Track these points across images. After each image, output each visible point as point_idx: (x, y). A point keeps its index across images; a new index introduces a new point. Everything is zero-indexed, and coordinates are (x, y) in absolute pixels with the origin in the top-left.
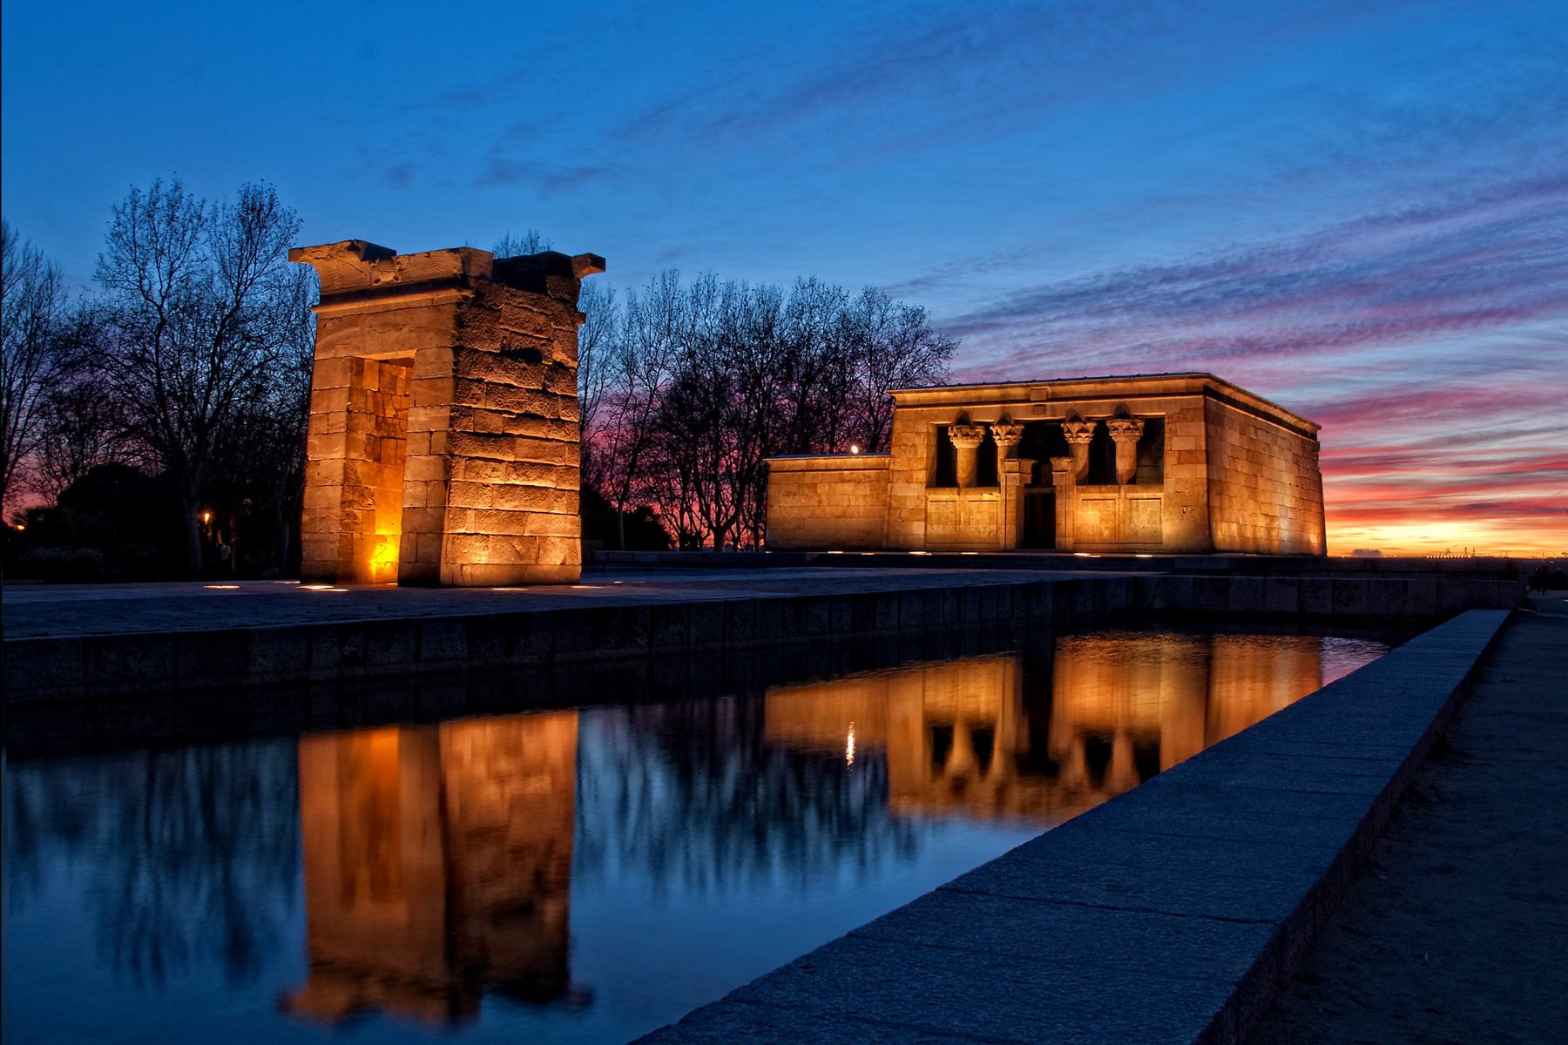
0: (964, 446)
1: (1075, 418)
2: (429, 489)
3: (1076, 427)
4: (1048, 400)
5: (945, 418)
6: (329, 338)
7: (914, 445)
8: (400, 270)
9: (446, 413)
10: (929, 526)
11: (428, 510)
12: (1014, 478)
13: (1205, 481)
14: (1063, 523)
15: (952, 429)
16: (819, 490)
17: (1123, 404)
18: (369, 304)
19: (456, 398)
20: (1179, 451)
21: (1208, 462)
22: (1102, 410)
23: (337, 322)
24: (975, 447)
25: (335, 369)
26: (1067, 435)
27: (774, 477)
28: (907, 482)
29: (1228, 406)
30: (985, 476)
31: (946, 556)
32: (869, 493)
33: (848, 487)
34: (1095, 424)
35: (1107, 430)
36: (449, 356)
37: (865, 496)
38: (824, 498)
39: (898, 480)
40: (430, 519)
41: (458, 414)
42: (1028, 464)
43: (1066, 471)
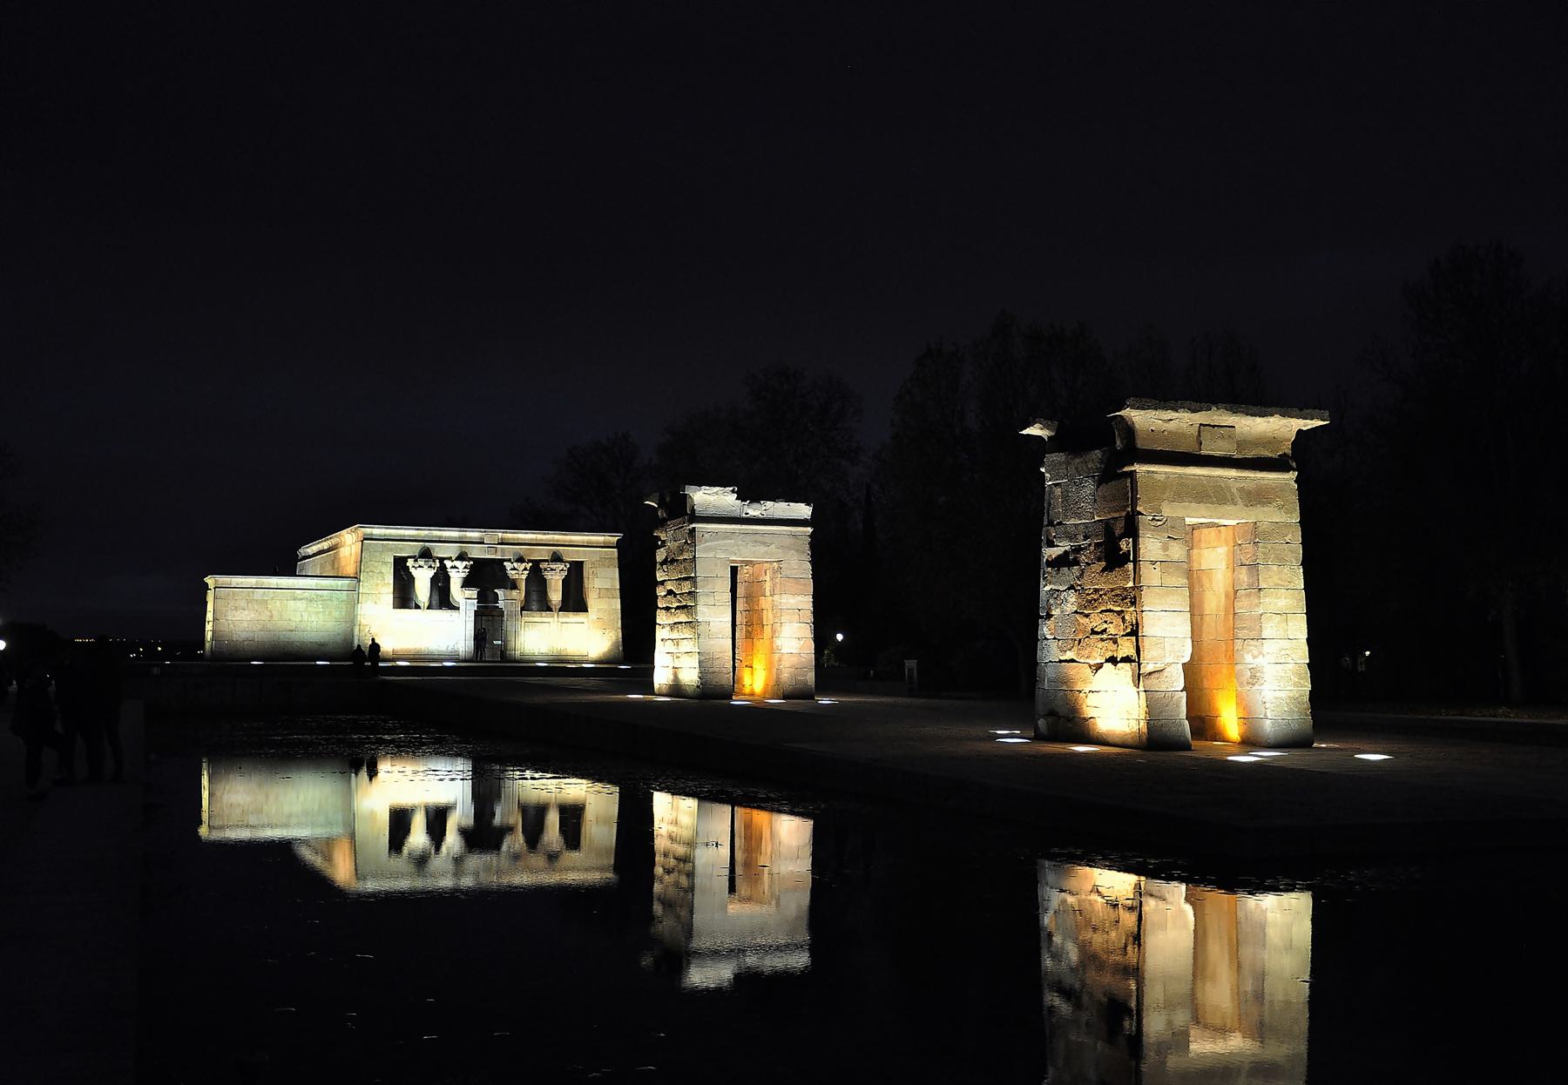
0: (423, 577)
1: (521, 560)
2: (802, 642)
4: (499, 544)
6: (707, 544)
12: (474, 604)
14: (513, 639)
15: (416, 561)
18: (744, 527)
22: (542, 553)
25: (716, 565)
30: (442, 598)
32: (321, 610)
33: (299, 603)
34: (531, 564)
37: (318, 613)
39: (366, 601)
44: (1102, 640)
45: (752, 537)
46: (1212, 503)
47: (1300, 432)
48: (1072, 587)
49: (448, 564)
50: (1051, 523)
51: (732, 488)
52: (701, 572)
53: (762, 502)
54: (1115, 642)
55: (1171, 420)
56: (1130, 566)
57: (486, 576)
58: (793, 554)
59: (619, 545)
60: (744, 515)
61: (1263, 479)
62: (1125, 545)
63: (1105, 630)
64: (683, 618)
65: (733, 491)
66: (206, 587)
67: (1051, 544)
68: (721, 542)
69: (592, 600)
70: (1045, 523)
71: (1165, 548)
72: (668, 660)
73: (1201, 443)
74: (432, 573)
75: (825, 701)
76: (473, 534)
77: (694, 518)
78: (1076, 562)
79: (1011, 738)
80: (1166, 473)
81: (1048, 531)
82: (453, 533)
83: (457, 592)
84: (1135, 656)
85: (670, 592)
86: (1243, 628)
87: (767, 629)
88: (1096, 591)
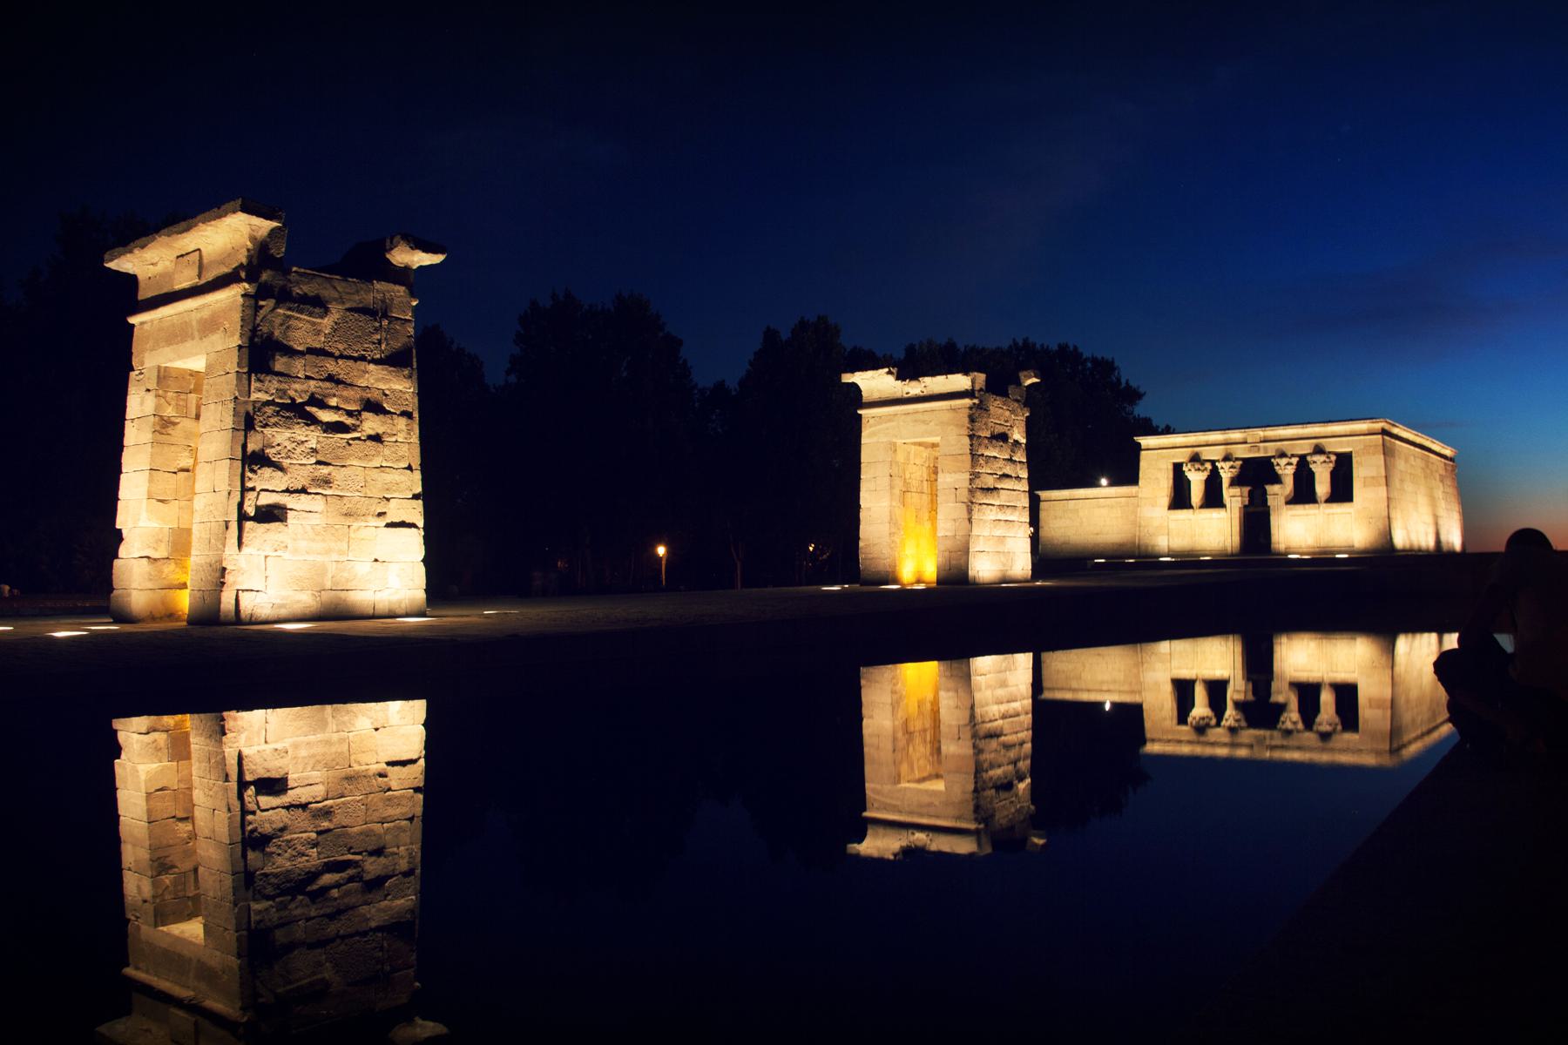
1: (1283, 455)
2: (957, 524)
3: (1283, 461)
4: (1261, 442)
5: (1182, 456)
6: (873, 429)
7: (1157, 479)
8: (925, 387)
9: (967, 476)
10: (1171, 540)
11: (957, 537)
13: (1386, 499)
16: (1081, 514)
17: (1321, 444)
19: (973, 467)
20: (1365, 478)
21: (1387, 485)
22: (1304, 448)
23: (877, 419)
24: (1205, 478)
26: (1277, 468)
27: (1042, 504)
28: (1153, 506)
29: (1398, 442)
30: (1213, 498)
31: (1188, 562)
35: (1308, 463)
36: (967, 440)
38: (1084, 520)
40: (958, 542)
41: (975, 476)
42: (1246, 490)
43: (1277, 494)
45: (909, 418)
51: (887, 370)
53: (921, 379)
58: (952, 430)
60: (906, 396)
61: (217, 302)
65: (890, 373)
68: (884, 426)
74: (1203, 476)
76: (1236, 435)
80: (152, 321)
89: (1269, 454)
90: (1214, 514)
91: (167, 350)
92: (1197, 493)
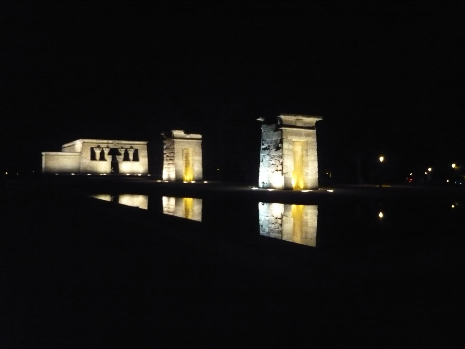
0: (98, 152)
1: (122, 148)
3: (123, 150)
5: (93, 146)
20: (143, 156)
22: (128, 146)
30: (102, 158)
44: (275, 166)
46: (298, 136)
47: (317, 121)
48: (268, 155)
49: (104, 149)
50: (263, 140)
51: (182, 131)
52: (176, 151)
54: (277, 166)
55: (290, 118)
56: (281, 150)
57: (114, 152)
59: (147, 145)
60: (186, 137)
61: (309, 131)
62: (280, 145)
63: (275, 164)
64: (171, 162)
65: (183, 132)
66: (42, 155)
67: (263, 145)
69: (141, 158)
70: (262, 140)
71: (288, 146)
72: (167, 173)
73: (296, 123)
75: (205, 182)
76: (110, 142)
77: (174, 138)
78: (269, 149)
79: (254, 188)
80: (289, 130)
81: (262, 143)
82: (105, 141)
83: (106, 156)
84: (282, 170)
85: (167, 156)
86: (304, 164)
87: (191, 165)
88: (273, 155)
89: (119, 147)
90: (103, 163)
91: (294, 137)
92: (98, 156)
